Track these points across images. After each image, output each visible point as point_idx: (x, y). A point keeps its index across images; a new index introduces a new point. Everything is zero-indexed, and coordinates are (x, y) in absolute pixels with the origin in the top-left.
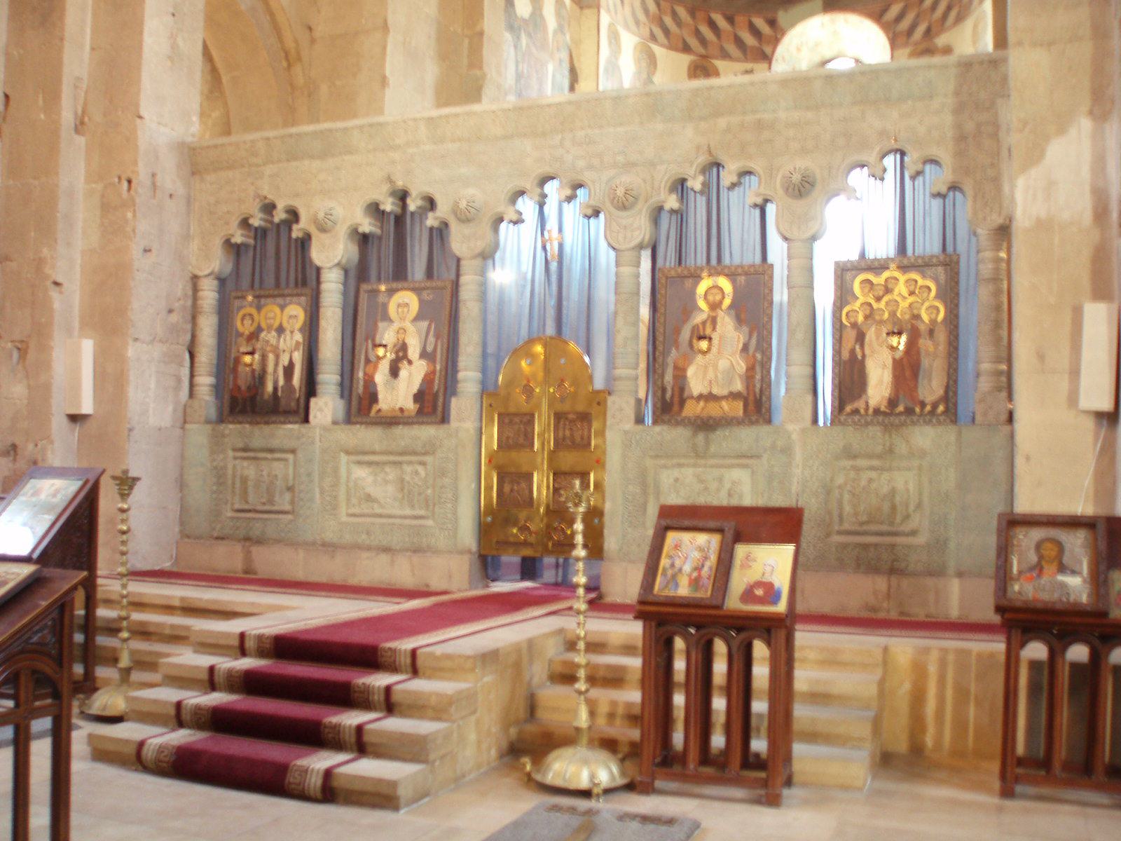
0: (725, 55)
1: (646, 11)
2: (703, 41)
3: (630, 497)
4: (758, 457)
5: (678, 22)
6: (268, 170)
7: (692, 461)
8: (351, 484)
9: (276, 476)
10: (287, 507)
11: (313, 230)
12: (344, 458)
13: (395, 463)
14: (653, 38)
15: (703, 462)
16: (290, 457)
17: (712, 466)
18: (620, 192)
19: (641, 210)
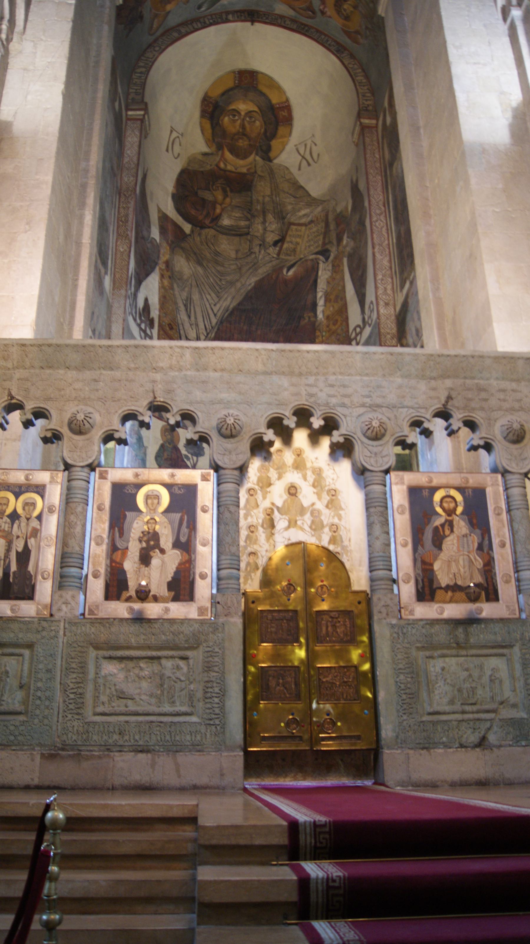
3: (403, 686)
4: (511, 646)
6: (18, 374)
7: (454, 652)
8: (101, 681)
9: (7, 672)
10: (18, 707)
11: (65, 431)
12: (92, 653)
13: (152, 658)
15: (464, 652)
16: (27, 653)
17: (472, 656)
18: (376, 424)
19: (388, 441)
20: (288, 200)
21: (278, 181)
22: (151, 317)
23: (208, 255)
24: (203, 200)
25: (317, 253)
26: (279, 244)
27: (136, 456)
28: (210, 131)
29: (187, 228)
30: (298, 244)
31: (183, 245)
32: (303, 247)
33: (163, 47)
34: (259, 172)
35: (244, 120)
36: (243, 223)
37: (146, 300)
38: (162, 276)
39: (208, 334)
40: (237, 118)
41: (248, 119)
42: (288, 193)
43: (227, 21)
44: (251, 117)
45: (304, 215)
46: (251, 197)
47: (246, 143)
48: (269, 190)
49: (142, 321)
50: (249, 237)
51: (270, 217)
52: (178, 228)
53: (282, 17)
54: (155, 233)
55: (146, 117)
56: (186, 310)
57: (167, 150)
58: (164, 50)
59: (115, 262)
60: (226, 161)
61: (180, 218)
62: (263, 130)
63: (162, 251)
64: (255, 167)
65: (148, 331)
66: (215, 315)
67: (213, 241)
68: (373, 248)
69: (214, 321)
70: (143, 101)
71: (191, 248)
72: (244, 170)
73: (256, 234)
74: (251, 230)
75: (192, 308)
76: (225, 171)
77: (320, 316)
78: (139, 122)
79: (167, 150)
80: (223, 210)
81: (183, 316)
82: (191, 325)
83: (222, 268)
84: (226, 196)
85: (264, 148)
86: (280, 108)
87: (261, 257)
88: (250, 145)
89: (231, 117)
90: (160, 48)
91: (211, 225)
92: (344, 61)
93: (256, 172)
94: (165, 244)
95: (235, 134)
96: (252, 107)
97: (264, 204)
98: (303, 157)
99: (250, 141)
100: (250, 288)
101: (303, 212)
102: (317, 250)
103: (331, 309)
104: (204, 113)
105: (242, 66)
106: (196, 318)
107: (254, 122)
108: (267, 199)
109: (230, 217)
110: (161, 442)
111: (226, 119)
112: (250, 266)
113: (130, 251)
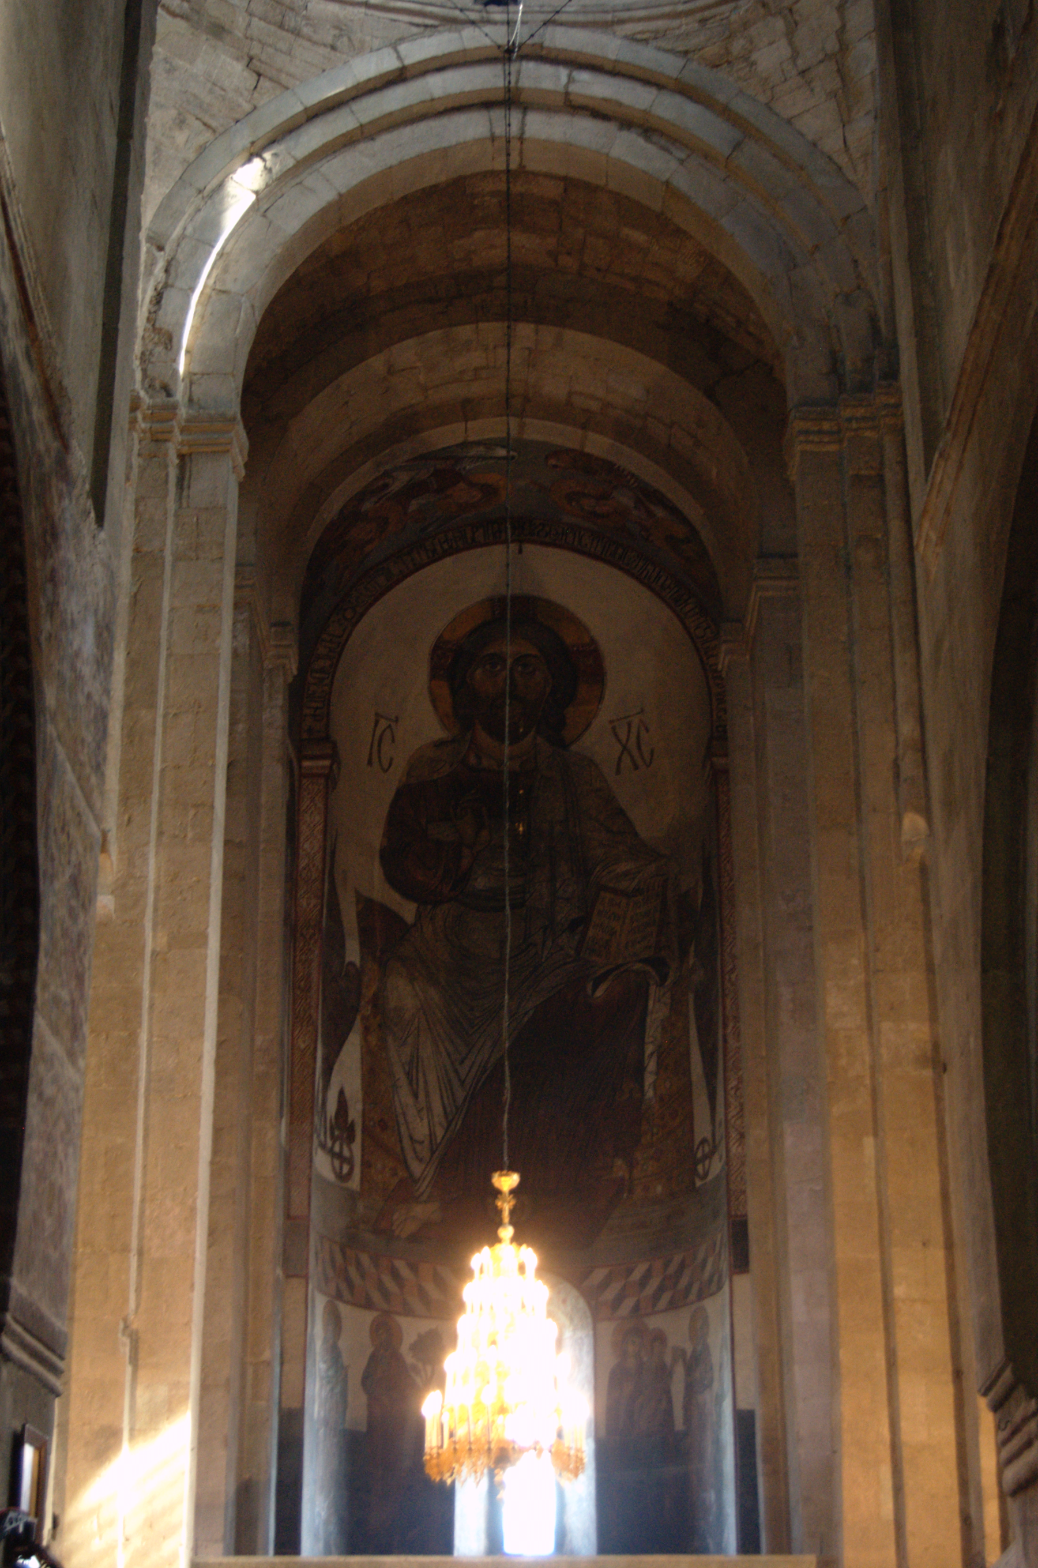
0: (409, 1312)
1: (333, 1261)
2: (386, 1294)
5: (363, 1276)
14: (339, 1296)
22: (350, 1120)
26: (581, 928)
27: (332, 1389)
29: (408, 911)
37: (341, 1093)
38: (366, 1031)
39: (449, 1126)
41: (520, 669)
43: (474, 545)
49: (334, 1139)
52: (391, 917)
54: (353, 952)
55: (334, 767)
56: (410, 1083)
57: (370, 763)
58: (362, 615)
59: (292, 1072)
61: (396, 897)
65: (346, 1153)
66: (462, 1083)
68: (725, 1026)
69: (460, 1095)
70: (327, 739)
75: (421, 1075)
77: (650, 1093)
78: (322, 781)
81: (404, 1096)
82: (419, 1111)
98: (625, 748)
100: (526, 1019)
101: (623, 867)
103: (668, 1084)
104: (434, 674)
106: (427, 1095)
110: (370, 1350)
111: (479, 672)
113: (315, 1048)
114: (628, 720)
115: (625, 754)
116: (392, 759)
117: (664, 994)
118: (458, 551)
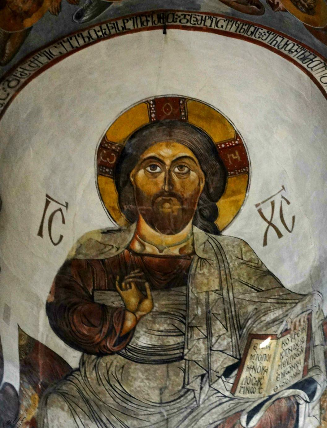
20: (248, 297)
21: (231, 265)
23: (111, 401)
24: (104, 307)
25: (295, 386)
26: (235, 372)
28: (115, 195)
30: (265, 370)
31: (64, 388)
32: (273, 378)
33: (23, 81)
34: (200, 253)
35: (169, 171)
36: (172, 341)
40: (158, 169)
41: (176, 170)
42: (247, 284)
43: (126, 31)
44: (181, 167)
45: (274, 321)
46: (187, 296)
47: (178, 207)
48: (217, 280)
50: (183, 364)
51: (218, 327)
53: (212, 15)
57: (40, 234)
60: (143, 239)
61: (61, 343)
62: (202, 185)
63: (24, 403)
64: (193, 244)
67: (119, 377)
71: (79, 391)
72: (176, 251)
73: (194, 358)
74: (186, 351)
76: (141, 255)
79: (40, 234)
80: (137, 321)
83: (135, 423)
84: (143, 297)
85: (206, 213)
86: (226, 148)
87: (203, 396)
88: (183, 209)
89: (149, 169)
90: (19, 81)
91: (116, 349)
92: (313, 73)
93: (194, 253)
94: (30, 392)
95: (157, 196)
96: (183, 151)
97: (208, 304)
98: (270, 223)
99: (182, 204)
101: (271, 316)
102: (295, 381)
105: (160, 92)
107: (188, 172)
108: (213, 296)
109: (149, 332)
111: (141, 173)
112: (185, 413)
114: (272, 200)
115: (271, 228)
116: (61, 237)
117: (313, 408)
118: (110, 36)
